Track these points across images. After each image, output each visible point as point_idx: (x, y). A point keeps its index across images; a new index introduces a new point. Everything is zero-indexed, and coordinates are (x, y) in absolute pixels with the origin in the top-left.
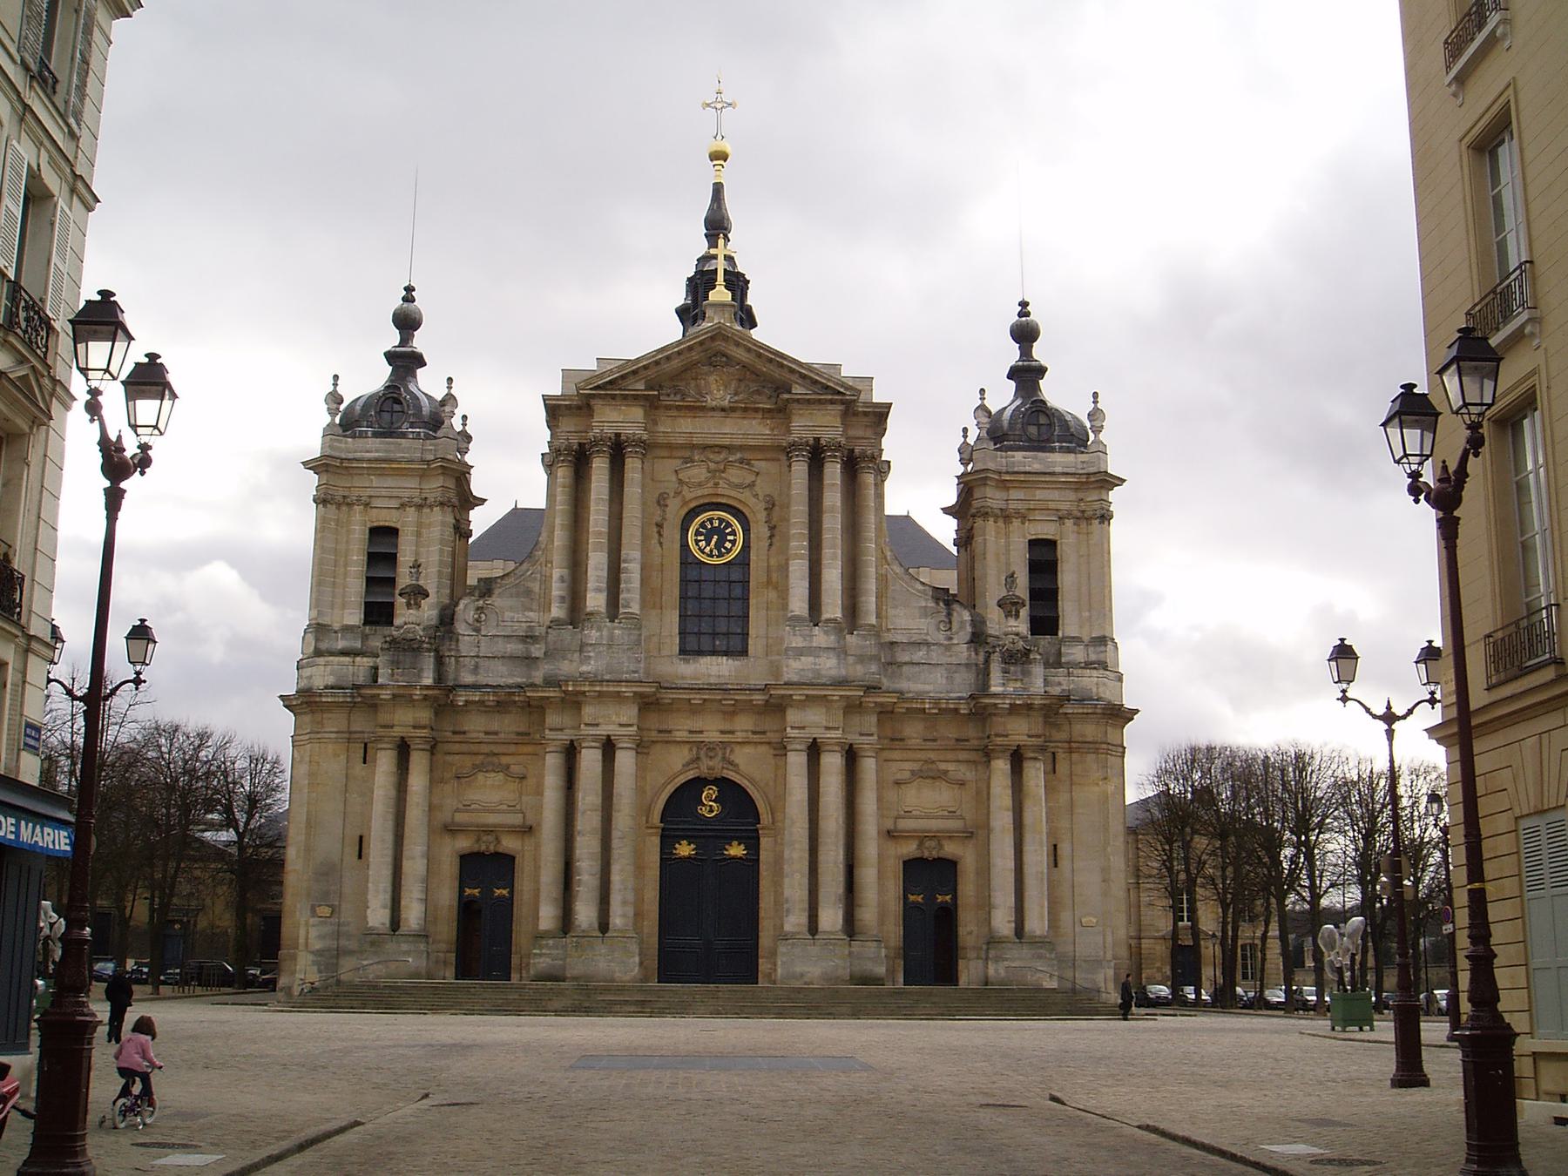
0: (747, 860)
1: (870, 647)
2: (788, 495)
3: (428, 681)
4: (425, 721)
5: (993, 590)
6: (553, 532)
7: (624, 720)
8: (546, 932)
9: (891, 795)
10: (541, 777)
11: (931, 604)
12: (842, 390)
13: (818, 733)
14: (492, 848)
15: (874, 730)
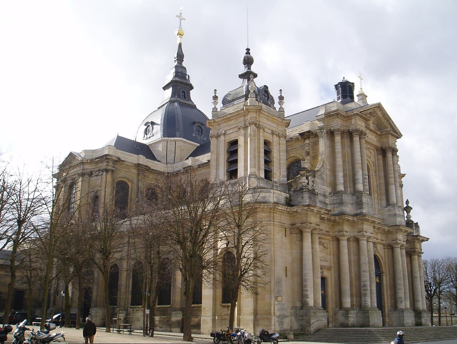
12: (399, 134)
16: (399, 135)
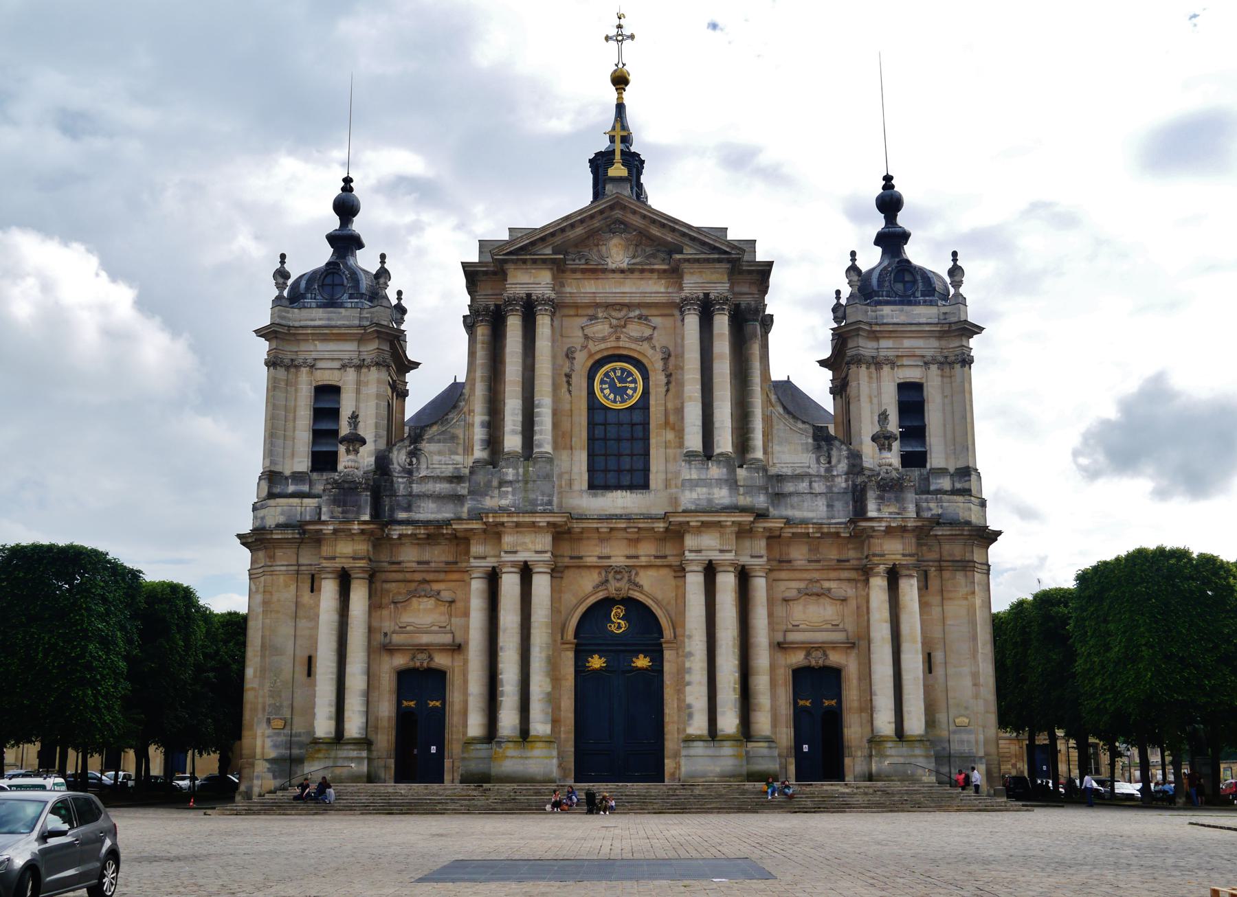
0: (653, 671)
1: (758, 479)
2: (683, 346)
3: (366, 517)
4: (363, 554)
5: (866, 427)
6: (474, 385)
7: (539, 548)
8: (474, 739)
9: (780, 611)
10: (468, 601)
11: (810, 440)
12: (728, 250)
13: (715, 556)
14: (425, 665)
15: (763, 552)
16: (726, 252)
